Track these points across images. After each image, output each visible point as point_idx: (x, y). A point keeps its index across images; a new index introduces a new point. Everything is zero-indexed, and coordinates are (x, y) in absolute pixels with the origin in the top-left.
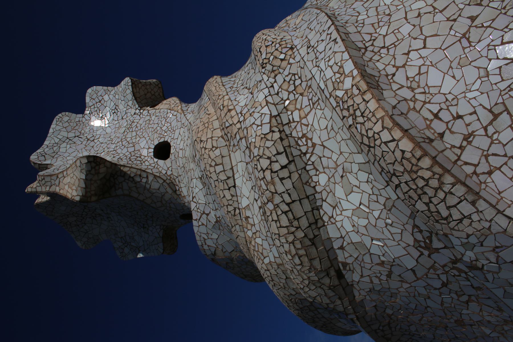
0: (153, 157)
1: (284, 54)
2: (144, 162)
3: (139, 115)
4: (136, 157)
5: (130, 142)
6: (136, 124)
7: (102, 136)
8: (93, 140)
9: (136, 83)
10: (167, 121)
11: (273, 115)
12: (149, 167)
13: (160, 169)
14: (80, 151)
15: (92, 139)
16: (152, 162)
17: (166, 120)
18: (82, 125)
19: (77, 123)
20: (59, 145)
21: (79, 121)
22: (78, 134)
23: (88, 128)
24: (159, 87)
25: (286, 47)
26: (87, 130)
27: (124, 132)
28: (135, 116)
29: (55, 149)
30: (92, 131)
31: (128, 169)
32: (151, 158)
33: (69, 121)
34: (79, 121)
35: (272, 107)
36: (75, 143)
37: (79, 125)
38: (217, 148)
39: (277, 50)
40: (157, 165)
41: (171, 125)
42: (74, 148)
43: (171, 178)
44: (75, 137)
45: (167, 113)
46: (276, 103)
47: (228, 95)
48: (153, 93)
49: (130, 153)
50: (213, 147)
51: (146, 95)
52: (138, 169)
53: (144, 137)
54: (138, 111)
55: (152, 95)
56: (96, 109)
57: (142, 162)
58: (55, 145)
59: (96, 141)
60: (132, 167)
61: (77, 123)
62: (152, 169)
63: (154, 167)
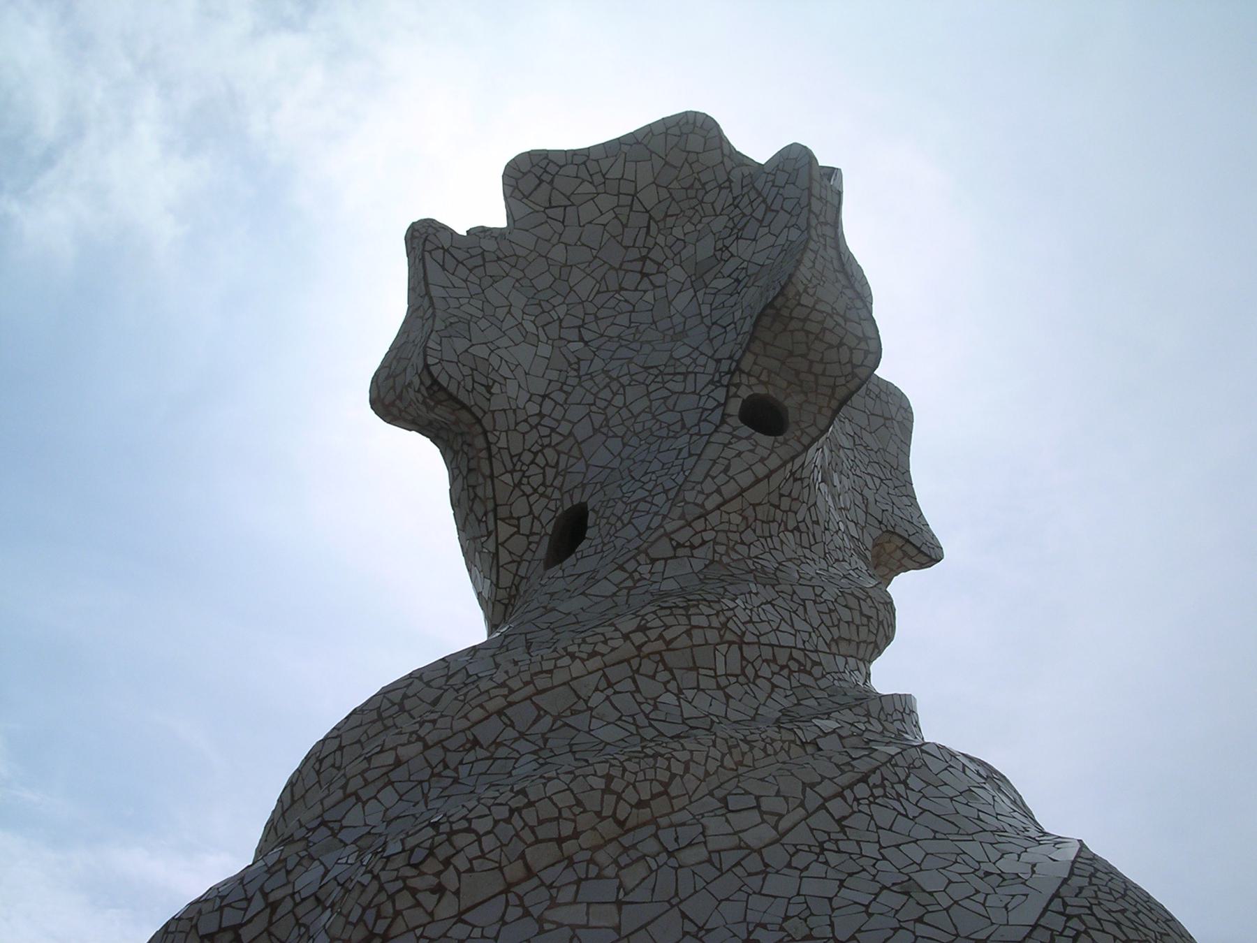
0: (560, 511)
1: (361, 919)
2: (542, 495)
3: (711, 382)
4: (552, 461)
5: (611, 411)
6: (678, 387)
7: (660, 292)
8: (644, 275)
9: (785, 312)
10: (643, 506)
11: (241, 931)
12: (525, 525)
13: (528, 556)
14: (597, 262)
15: (650, 267)
16: (547, 516)
17: (643, 499)
18: (695, 202)
19: (697, 185)
20: (601, 189)
21: (704, 185)
22: (658, 215)
23: (689, 228)
24: (854, 375)
25: (379, 916)
26: (678, 232)
27: (647, 368)
28: (711, 366)
29: (587, 188)
30: (676, 249)
31: (487, 472)
32: (556, 512)
33: (692, 157)
34: (704, 185)
35: (260, 924)
36: (624, 226)
37: (691, 193)
38: (318, 773)
39: (381, 888)
40: (536, 538)
41: (624, 526)
42: (606, 236)
43: (514, 596)
44: (647, 212)
45: (666, 492)
46: (273, 929)
47: (427, 747)
48: (818, 368)
49: (571, 433)
50: (321, 761)
51: (791, 354)
52: (494, 498)
53: (625, 445)
54: (725, 366)
55: (809, 371)
56: (748, 211)
57: (541, 490)
58: (598, 179)
59: (645, 284)
60: (492, 477)
61: (697, 185)
62: (518, 532)
63: (532, 534)
